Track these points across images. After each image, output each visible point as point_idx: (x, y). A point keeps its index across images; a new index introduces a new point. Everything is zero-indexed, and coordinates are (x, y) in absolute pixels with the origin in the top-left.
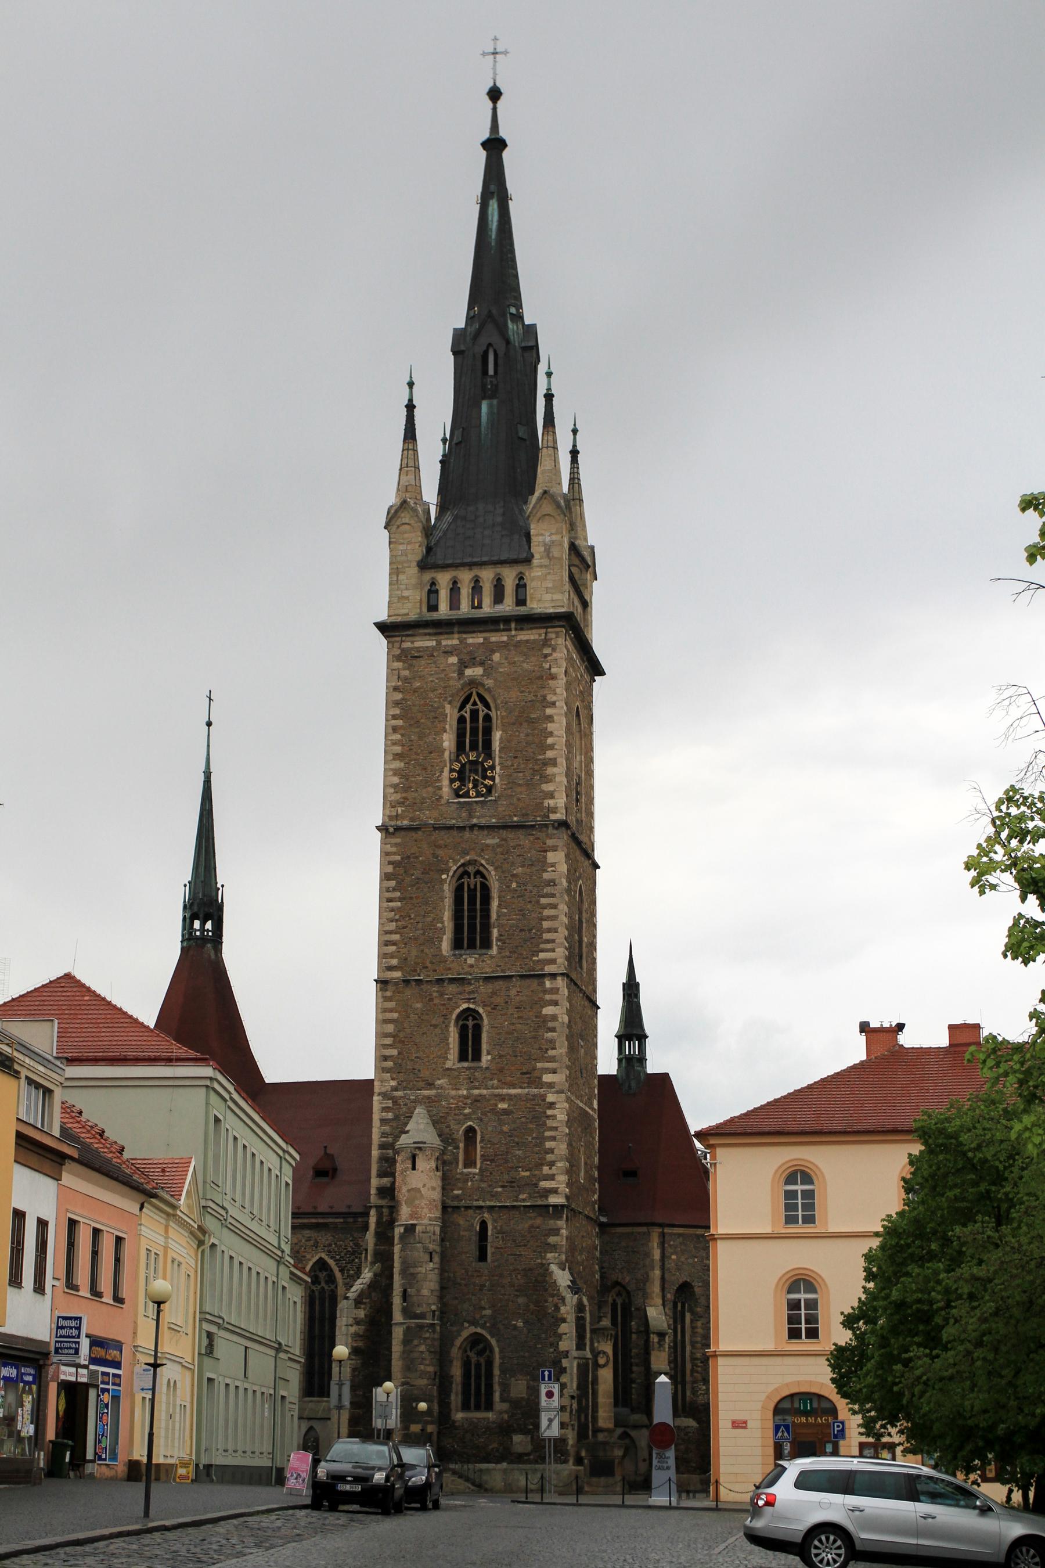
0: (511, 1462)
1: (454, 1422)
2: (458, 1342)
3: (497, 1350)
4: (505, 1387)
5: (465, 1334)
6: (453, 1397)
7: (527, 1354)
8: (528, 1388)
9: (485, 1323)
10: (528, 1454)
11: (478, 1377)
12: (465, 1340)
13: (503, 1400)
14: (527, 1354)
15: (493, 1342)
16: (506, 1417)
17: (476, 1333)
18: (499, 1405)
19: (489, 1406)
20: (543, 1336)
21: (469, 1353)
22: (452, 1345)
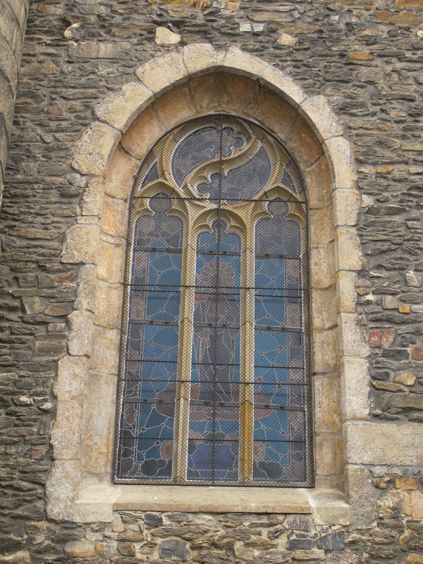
1: (68, 530)
2: (122, 105)
5: (161, 73)
6: (68, 380)
9: (272, 30)
11: (219, 295)
12: (159, 102)
15: (320, 112)
17: (220, 79)
19: (294, 457)
22: (86, 118)
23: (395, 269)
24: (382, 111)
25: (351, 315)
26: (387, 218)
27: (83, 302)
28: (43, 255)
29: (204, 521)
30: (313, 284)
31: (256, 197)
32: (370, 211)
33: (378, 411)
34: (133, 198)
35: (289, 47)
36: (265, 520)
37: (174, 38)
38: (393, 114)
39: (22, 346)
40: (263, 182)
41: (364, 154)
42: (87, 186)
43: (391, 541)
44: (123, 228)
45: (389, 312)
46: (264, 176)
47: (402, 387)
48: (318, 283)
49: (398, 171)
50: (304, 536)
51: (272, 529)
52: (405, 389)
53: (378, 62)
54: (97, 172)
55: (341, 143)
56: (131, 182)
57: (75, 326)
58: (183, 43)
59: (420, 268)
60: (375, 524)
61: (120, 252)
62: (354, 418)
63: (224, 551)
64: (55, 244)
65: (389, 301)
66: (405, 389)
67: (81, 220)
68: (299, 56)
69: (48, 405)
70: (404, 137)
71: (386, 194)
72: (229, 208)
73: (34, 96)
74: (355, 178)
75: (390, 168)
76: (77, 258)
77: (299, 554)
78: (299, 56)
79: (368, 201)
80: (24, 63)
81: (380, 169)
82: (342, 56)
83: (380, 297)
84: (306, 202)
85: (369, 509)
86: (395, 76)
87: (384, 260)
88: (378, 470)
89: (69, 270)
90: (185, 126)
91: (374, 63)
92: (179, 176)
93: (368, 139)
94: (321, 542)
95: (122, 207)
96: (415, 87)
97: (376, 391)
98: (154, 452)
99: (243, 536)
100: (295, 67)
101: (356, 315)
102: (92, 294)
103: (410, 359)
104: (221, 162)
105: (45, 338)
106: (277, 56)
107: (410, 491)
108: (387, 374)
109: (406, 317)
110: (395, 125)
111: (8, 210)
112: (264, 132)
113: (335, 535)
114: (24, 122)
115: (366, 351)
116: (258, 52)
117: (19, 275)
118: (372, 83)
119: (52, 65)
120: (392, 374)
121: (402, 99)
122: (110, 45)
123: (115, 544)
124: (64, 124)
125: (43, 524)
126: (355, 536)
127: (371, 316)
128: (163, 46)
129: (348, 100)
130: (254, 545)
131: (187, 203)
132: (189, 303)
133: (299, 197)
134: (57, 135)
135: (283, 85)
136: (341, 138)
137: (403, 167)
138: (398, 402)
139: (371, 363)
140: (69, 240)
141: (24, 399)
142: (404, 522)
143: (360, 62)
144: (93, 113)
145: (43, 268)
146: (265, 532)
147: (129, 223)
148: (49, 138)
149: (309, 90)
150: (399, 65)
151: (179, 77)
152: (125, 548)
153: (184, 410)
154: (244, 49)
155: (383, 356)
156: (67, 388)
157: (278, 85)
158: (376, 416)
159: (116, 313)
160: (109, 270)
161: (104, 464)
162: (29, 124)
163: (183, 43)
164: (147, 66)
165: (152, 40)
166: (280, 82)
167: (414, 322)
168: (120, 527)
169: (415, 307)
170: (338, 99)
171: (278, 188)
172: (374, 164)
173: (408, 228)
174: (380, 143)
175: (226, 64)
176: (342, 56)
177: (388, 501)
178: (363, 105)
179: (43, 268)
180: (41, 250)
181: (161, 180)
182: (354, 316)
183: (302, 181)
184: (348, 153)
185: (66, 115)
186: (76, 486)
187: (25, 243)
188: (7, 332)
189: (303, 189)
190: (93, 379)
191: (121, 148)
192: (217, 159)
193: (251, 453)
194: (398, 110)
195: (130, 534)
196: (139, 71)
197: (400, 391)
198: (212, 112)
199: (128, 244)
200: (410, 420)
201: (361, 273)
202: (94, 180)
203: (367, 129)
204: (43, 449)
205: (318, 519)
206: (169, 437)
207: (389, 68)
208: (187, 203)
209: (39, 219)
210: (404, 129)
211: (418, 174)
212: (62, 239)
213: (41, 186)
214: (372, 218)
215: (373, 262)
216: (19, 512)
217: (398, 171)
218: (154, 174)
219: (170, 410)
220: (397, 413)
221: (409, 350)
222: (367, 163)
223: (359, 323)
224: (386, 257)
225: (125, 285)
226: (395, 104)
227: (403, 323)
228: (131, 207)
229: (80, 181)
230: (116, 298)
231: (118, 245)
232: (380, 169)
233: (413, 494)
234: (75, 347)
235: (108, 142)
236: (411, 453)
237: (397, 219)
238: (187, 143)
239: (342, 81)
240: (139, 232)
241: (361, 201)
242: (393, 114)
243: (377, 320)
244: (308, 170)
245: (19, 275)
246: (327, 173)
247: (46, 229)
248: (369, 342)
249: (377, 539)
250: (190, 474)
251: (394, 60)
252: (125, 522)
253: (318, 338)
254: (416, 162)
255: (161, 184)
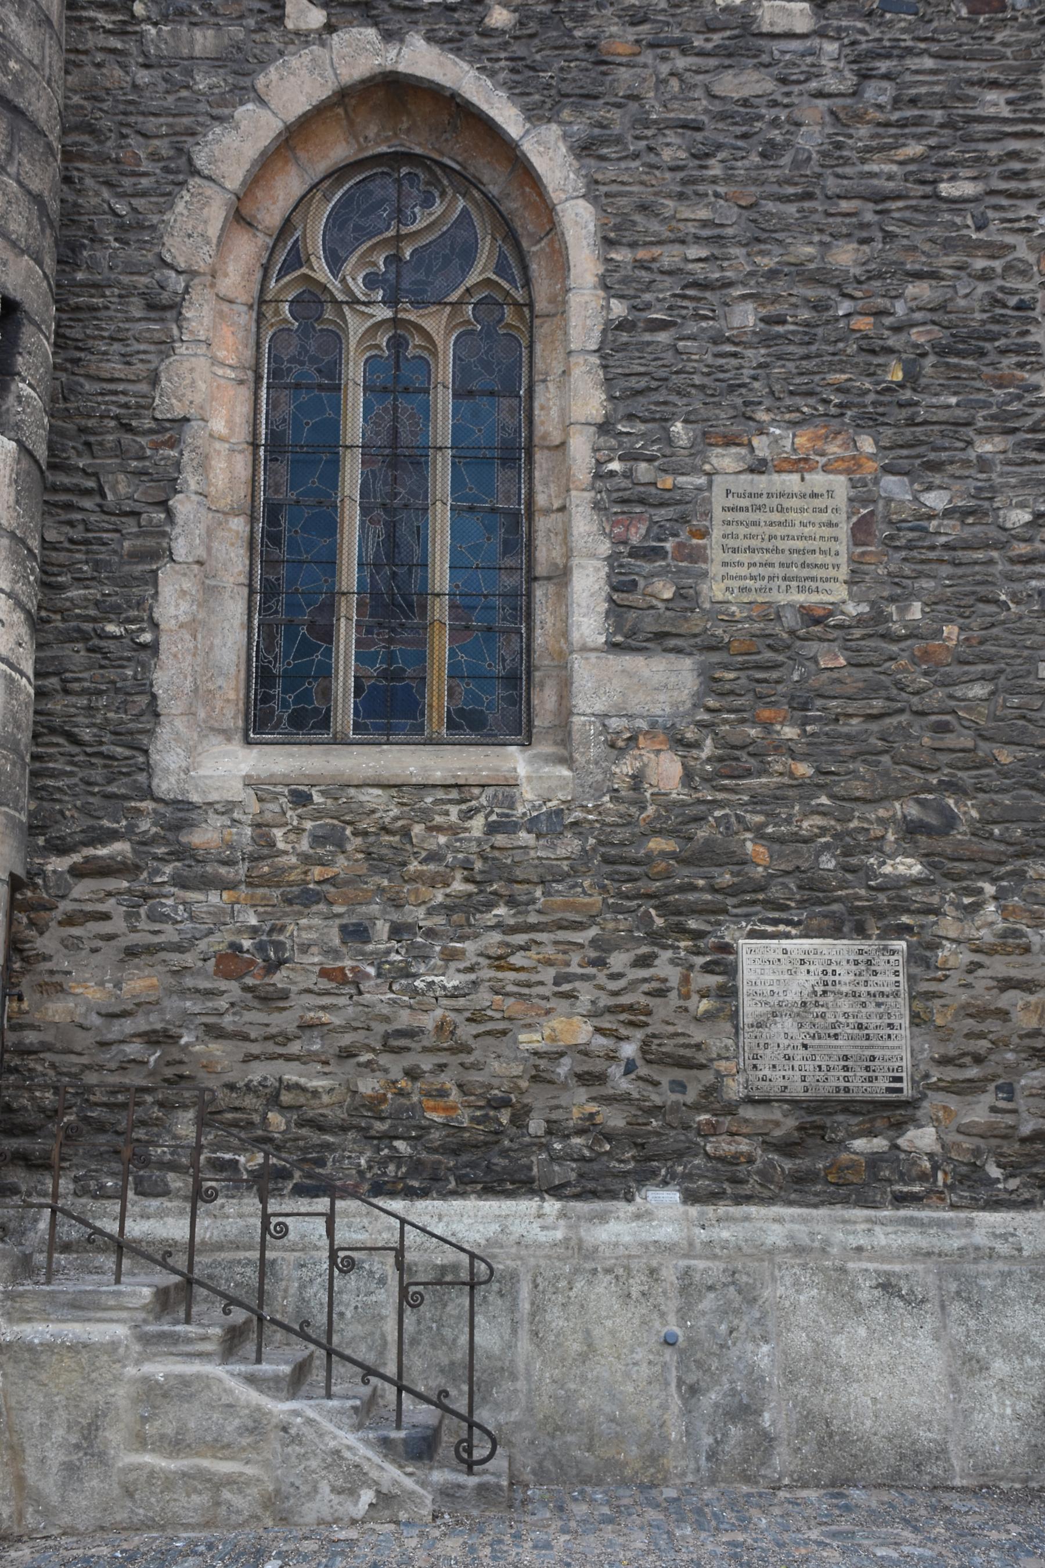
0: (723, 1184)
1: (182, 814)
2: (234, 147)
3: (579, 221)
4: (655, 526)
5: (296, 86)
6: (173, 601)
7: (846, 257)
8: (861, 531)
10: (893, 1112)
11: (398, 459)
13: (633, 631)
14: (846, 257)
15: (549, 155)
16: (667, 771)
17: (394, 91)
18: (609, 685)
19: (502, 701)
20: (995, 102)
21: (321, 271)
23: (654, 420)
24: (650, 149)
25: (586, 494)
26: (647, 337)
27: (191, 480)
28: (126, 406)
29: (372, 797)
30: (536, 440)
31: (454, 297)
32: (623, 325)
33: (619, 639)
34: (262, 301)
35: (504, 32)
36: (454, 794)
37: (317, 18)
38: (667, 154)
39: (103, 548)
40: (465, 271)
41: (617, 228)
42: (186, 291)
43: (629, 822)
44: (249, 353)
45: (642, 489)
46: (468, 256)
47: (655, 602)
48: (544, 438)
49: (669, 256)
50: (507, 816)
51: (464, 807)
52: (660, 605)
53: (648, 57)
54: (202, 267)
55: (581, 211)
56: (258, 275)
57: (180, 519)
58: (330, 28)
59: (692, 418)
60: (607, 798)
61: (245, 393)
62: (584, 649)
63: (397, 838)
64: (143, 387)
65: (643, 470)
66: (660, 605)
67: (181, 349)
68: (519, 49)
69: (147, 637)
70: (681, 196)
71: (648, 297)
72: (412, 317)
73: (92, 130)
74: (601, 271)
75: (656, 251)
76: (179, 412)
77: (500, 840)
78: (519, 49)
79: (619, 309)
80: (71, 67)
81: (642, 254)
82: (590, 47)
83: (629, 464)
84: (531, 305)
85: (600, 777)
86: (674, 83)
87: (639, 405)
88: (614, 723)
89: (167, 430)
90: (339, 174)
91: (641, 59)
92: (335, 262)
93: (622, 201)
94: (532, 825)
95: (246, 318)
96: (704, 102)
97: (616, 611)
98: (305, 697)
99: (425, 816)
100: (513, 70)
101: (593, 494)
102: (203, 466)
103: (669, 560)
104: (399, 238)
105: (137, 535)
106: (484, 51)
107: (658, 752)
108: (634, 583)
109: (667, 495)
110: (668, 175)
111: (68, 332)
112: (466, 182)
113: (550, 814)
114: (81, 179)
115: (605, 548)
116: (453, 44)
117: (92, 439)
118: (636, 98)
119: (118, 72)
120: (642, 583)
121: (683, 127)
122: (210, 33)
123: (249, 831)
124: (145, 182)
125: (148, 805)
126: (578, 814)
127: (615, 495)
128: (297, 33)
129: (597, 131)
130: (439, 829)
131: (346, 309)
132: (352, 474)
133: (519, 295)
134: (135, 202)
135: (492, 105)
136: (581, 202)
137: (677, 249)
138: (649, 624)
139: (611, 567)
140: (164, 382)
141: (111, 628)
142: (648, 795)
143: (618, 60)
144: (190, 161)
145: (128, 428)
146: (454, 810)
147: (258, 345)
148: (121, 208)
149: (534, 115)
150: (681, 62)
151: (325, 93)
152: (261, 836)
153: (346, 636)
154: (430, 38)
155: (630, 555)
156: (172, 611)
157: (485, 107)
158: (616, 645)
159: (243, 491)
160: (230, 423)
161: (232, 717)
162: (89, 182)
163: (330, 28)
164: (273, 72)
165: (279, 20)
166: (488, 101)
167: (679, 503)
168: (255, 807)
169: (681, 479)
170: (580, 128)
171: (488, 280)
172: (633, 245)
173: (678, 352)
174: (643, 208)
175: (401, 68)
176: (590, 47)
177: (626, 767)
178: (618, 140)
179: (128, 428)
180: (123, 399)
181: (304, 270)
182: (589, 495)
183: (525, 268)
184: (591, 227)
185: (146, 166)
186: (191, 751)
187: (97, 387)
188: (81, 527)
189: (527, 283)
190: (210, 592)
191: (240, 217)
192: (391, 233)
193: (438, 697)
194: (673, 149)
195: (268, 817)
196: (261, 81)
197: (652, 607)
198: (384, 149)
199: (258, 378)
200: (665, 650)
201: (604, 428)
202: (196, 281)
203: (623, 183)
204: (143, 700)
205: (528, 793)
206: (326, 672)
207: (664, 69)
208: (346, 309)
209: (117, 346)
210: (684, 182)
211: (700, 260)
212: (154, 380)
213: (116, 291)
214: (624, 337)
215: (622, 410)
216: (112, 789)
217: (669, 256)
218: (297, 259)
219: (327, 634)
220: (647, 640)
221: (669, 546)
222: (620, 244)
223: (597, 506)
224: (642, 400)
225: (255, 445)
226: (671, 137)
227: (662, 505)
228: (260, 317)
229: (178, 283)
230: (242, 466)
231: (241, 382)
232: (642, 254)
233: (662, 755)
234: (181, 549)
235: (216, 214)
236: (662, 697)
237: (663, 337)
238: (346, 202)
239: (588, 96)
240: (274, 358)
241: (608, 308)
242: (667, 154)
243: (624, 501)
244: (534, 249)
245: (92, 439)
246: (561, 264)
247: (128, 363)
248: (609, 536)
249: (609, 820)
250: (357, 727)
251: (674, 53)
252: (260, 800)
253: (542, 524)
254: (697, 239)
255: (306, 277)
